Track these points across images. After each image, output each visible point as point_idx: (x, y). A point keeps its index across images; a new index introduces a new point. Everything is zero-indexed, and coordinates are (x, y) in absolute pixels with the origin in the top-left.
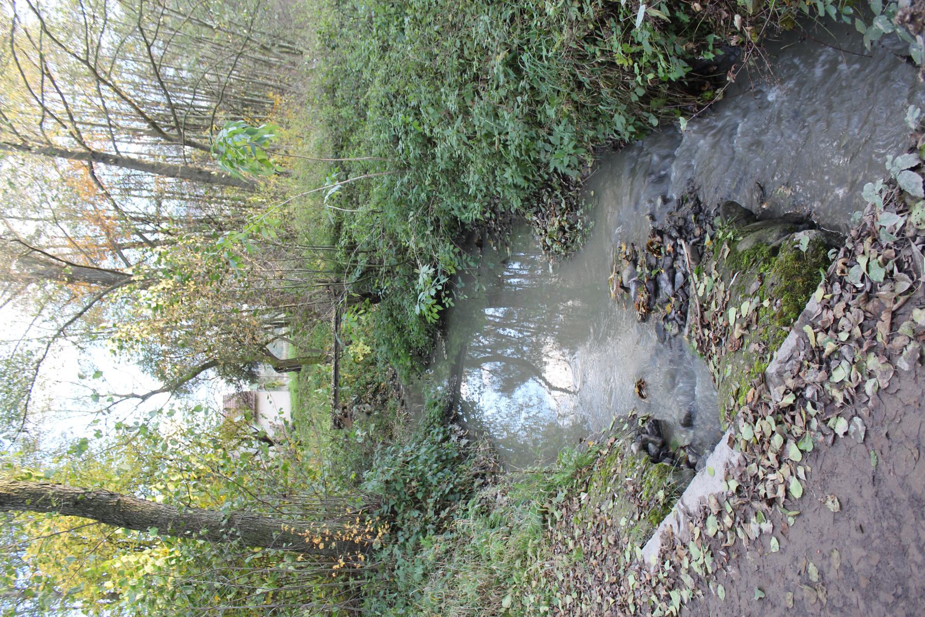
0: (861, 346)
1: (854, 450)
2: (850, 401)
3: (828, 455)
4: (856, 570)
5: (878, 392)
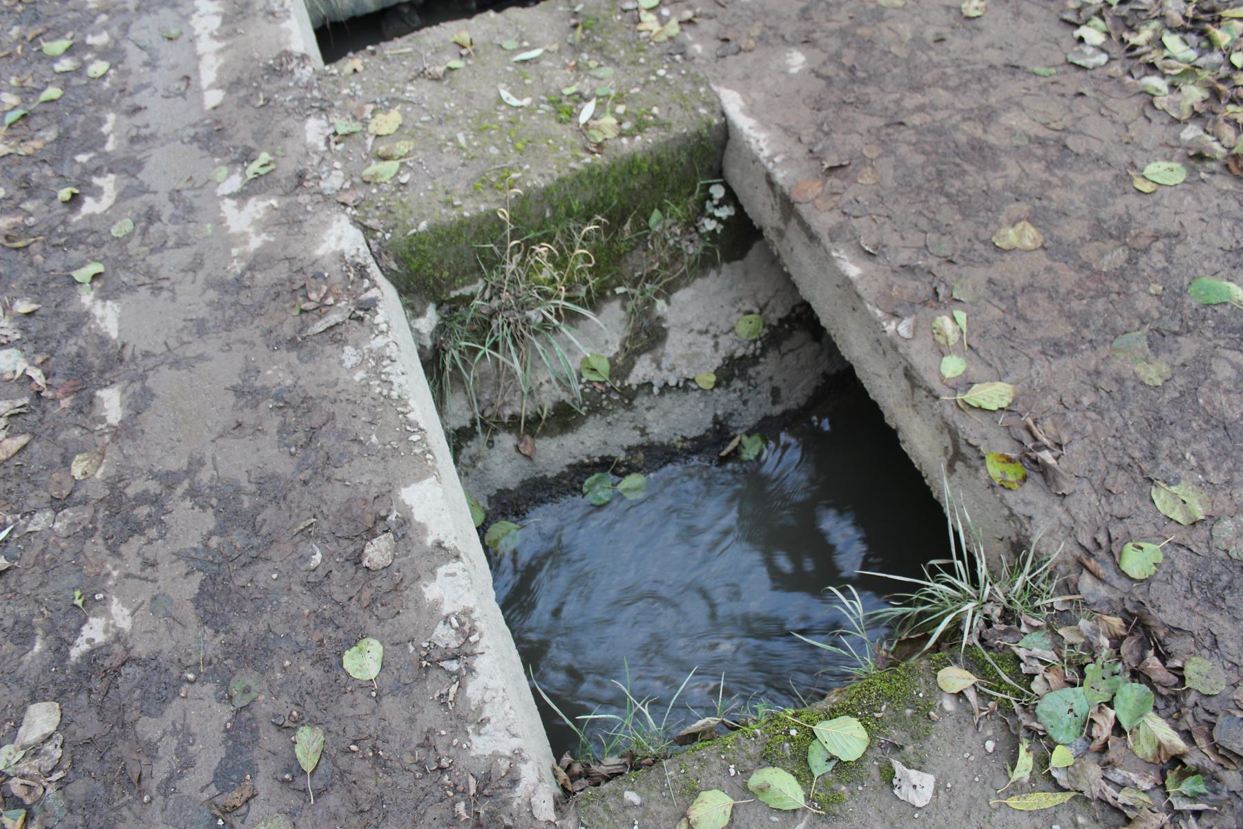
0: (1220, 80)
1: (1055, 47)
2: (1134, 53)
3: (1045, 12)
4: (879, 25)
5: (1146, 92)
